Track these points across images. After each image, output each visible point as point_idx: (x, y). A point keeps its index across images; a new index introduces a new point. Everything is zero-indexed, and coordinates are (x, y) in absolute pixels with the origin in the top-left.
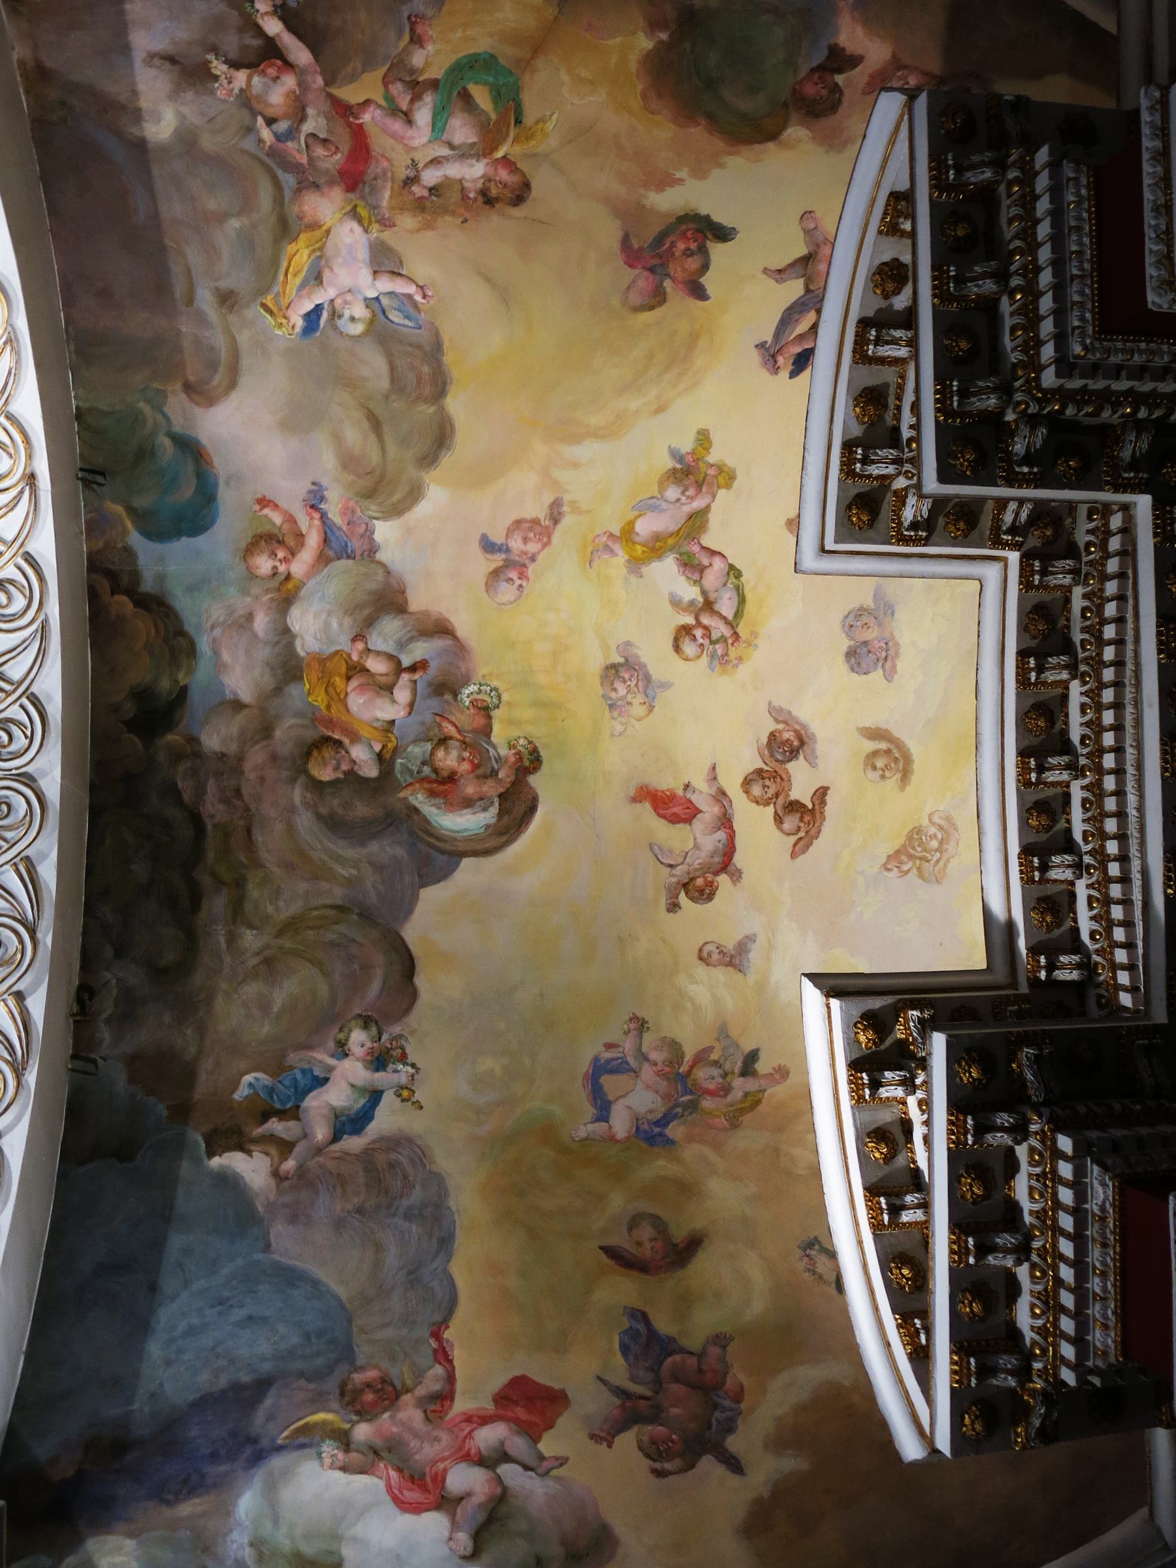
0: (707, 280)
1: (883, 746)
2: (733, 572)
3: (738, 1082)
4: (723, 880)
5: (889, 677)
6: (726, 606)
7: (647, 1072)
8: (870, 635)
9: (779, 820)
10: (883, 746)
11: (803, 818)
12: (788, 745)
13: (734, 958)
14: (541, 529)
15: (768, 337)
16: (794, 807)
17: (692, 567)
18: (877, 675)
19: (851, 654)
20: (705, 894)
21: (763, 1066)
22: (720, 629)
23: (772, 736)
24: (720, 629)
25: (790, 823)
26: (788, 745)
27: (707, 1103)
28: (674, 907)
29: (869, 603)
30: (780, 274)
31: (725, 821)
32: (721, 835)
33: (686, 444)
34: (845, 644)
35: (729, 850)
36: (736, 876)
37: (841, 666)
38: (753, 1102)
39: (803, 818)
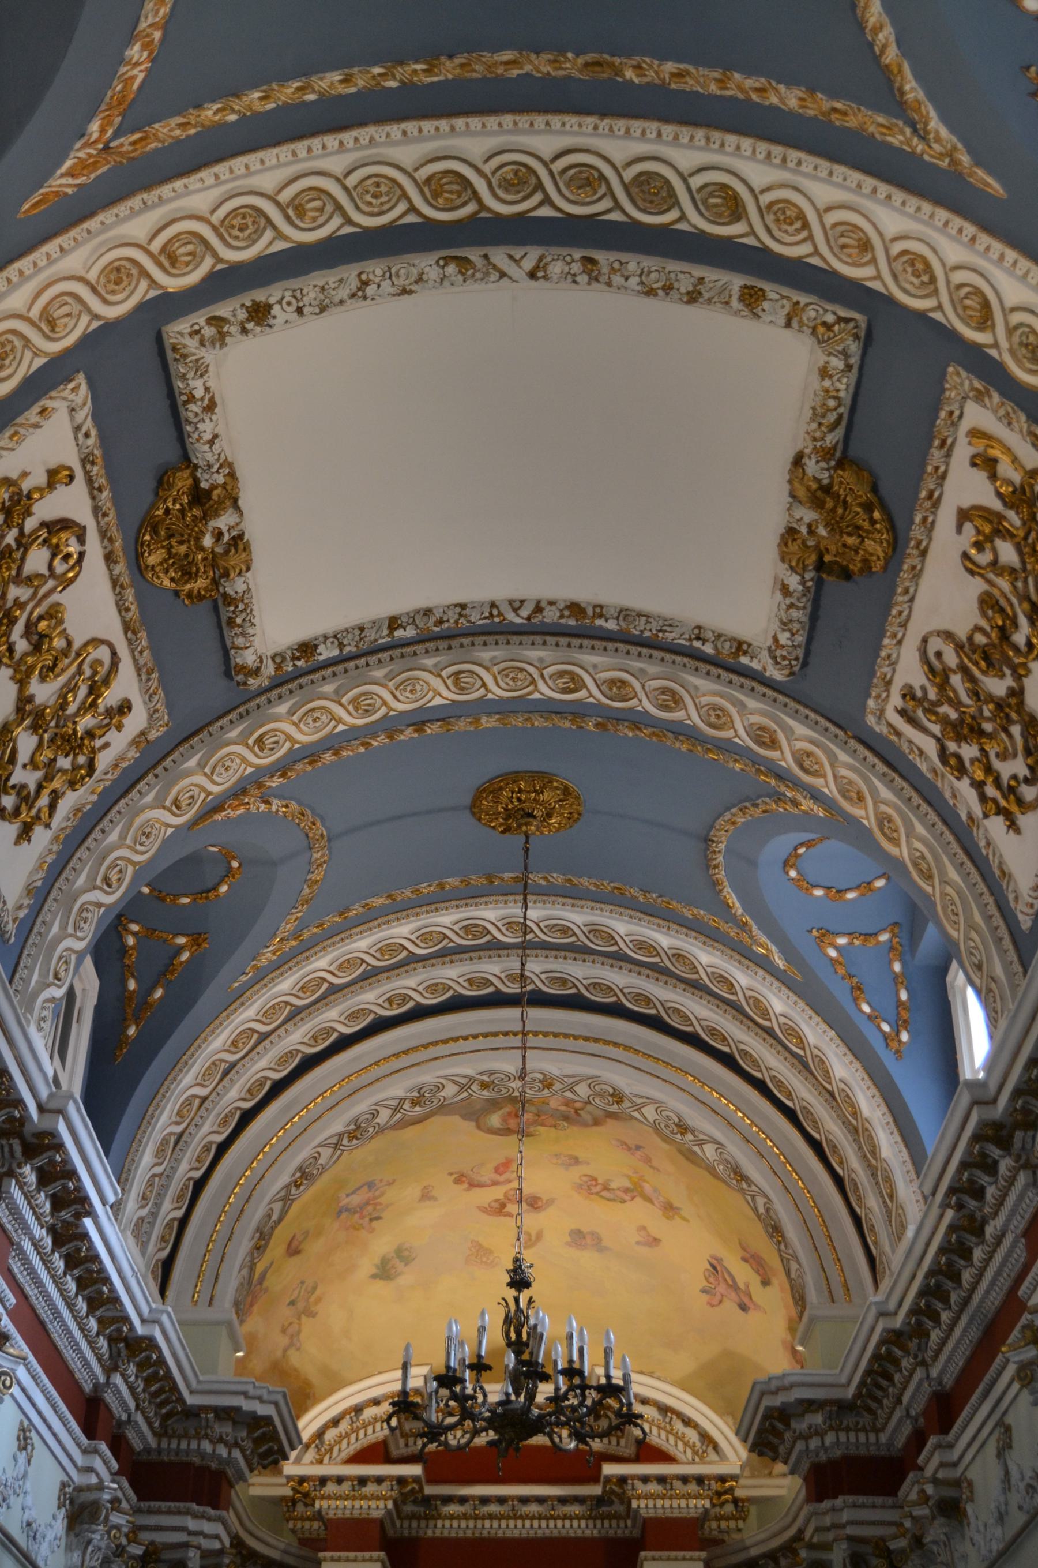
0: (746, 1265)
1: (533, 1238)
2: (623, 1201)
3: (367, 1219)
4: (465, 1186)
5: (568, 1244)
6: (605, 1194)
7: (370, 1194)
8: (589, 1241)
9: (496, 1201)
10: (533, 1238)
11: (500, 1209)
12: (534, 1204)
13: (426, 1196)
14: (648, 1160)
15: (725, 1264)
16: (503, 1206)
17: (626, 1190)
18: (569, 1239)
19: (579, 1232)
20: (457, 1181)
21: (375, 1224)
22: (594, 1190)
23: (540, 1198)
24: (594, 1190)
25: (496, 1205)
26: (534, 1204)
27: (357, 1216)
28: (451, 1174)
29: (604, 1244)
30: (747, 1286)
31: (495, 1183)
32: (489, 1182)
33: (683, 1213)
34: (585, 1230)
35: (480, 1185)
36: (468, 1190)
37: (574, 1227)
38: (357, 1228)
39: (500, 1209)
